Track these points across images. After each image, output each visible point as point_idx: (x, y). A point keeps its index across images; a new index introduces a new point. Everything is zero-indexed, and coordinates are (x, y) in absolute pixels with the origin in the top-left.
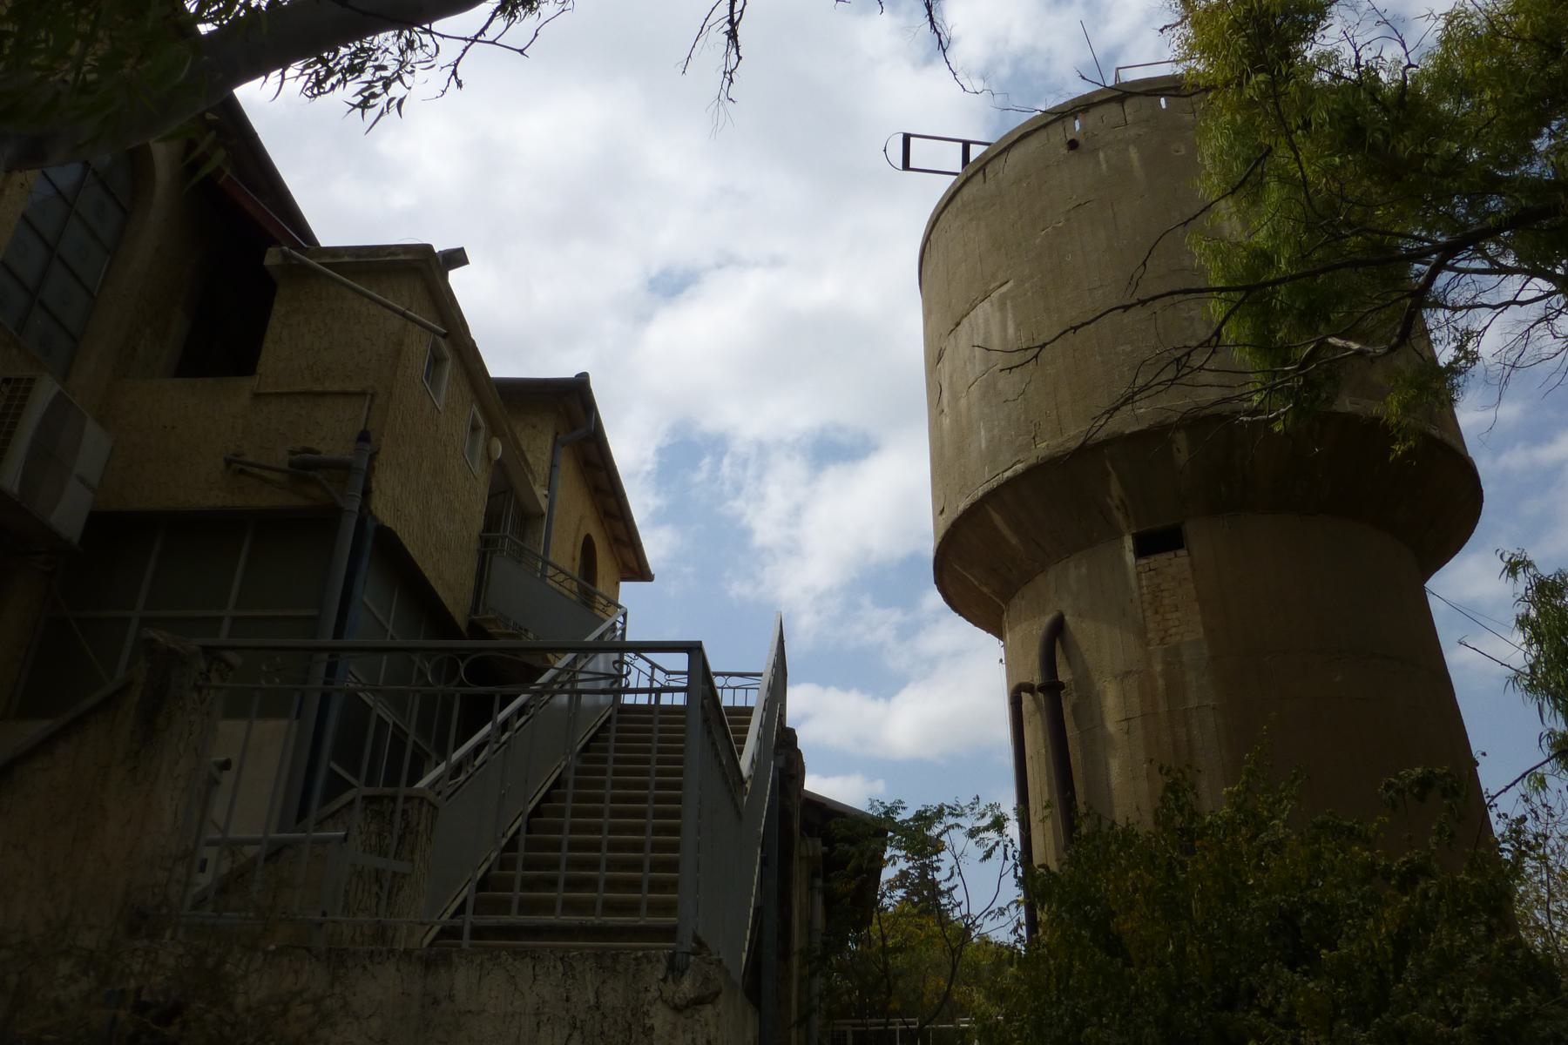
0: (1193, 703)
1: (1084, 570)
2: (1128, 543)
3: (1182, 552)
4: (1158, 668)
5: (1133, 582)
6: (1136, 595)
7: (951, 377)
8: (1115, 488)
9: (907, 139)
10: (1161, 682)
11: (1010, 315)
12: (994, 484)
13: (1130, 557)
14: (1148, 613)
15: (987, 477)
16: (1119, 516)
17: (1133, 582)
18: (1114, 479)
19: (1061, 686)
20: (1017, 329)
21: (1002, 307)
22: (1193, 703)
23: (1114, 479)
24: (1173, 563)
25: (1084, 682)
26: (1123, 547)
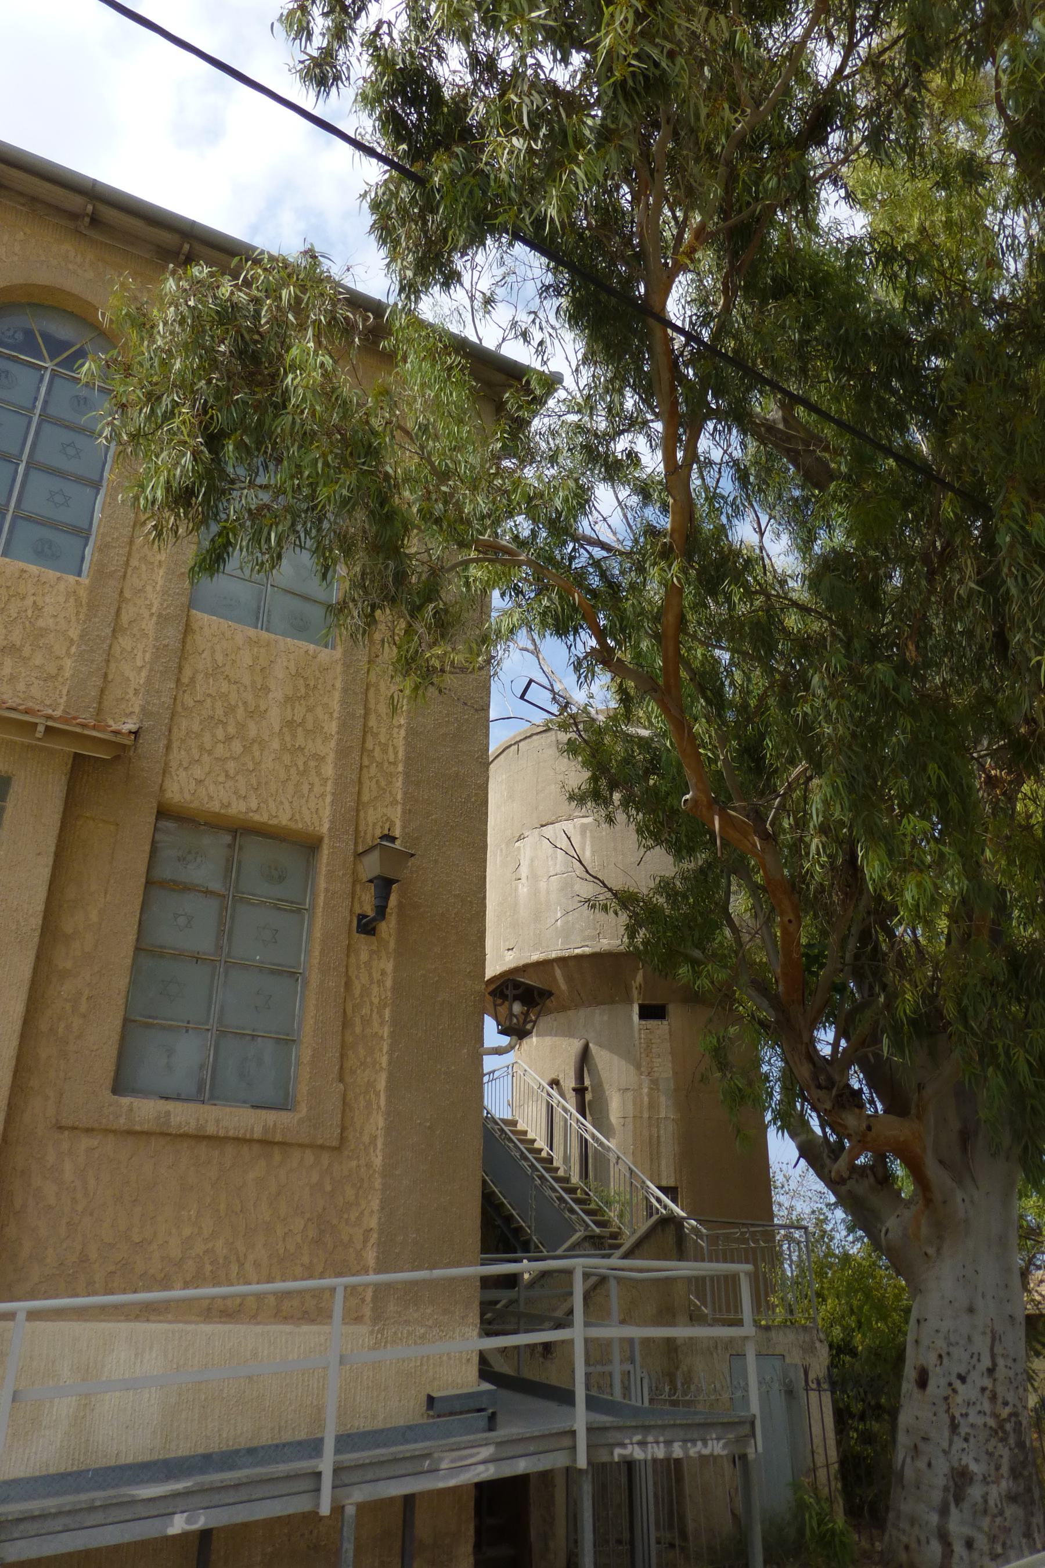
0: (663, 1115)
1: (606, 1018)
2: (636, 1009)
3: (665, 1022)
4: (646, 1090)
5: (636, 1035)
6: (637, 1042)
7: (532, 860)
8: (639, 977)
9: (531, 681)
10: (646, 1099)
11: (588, 842)
12: (566, 954)
13: (636, 1017)
14: (643, 1055)
15: (560, 947)
16: (635, 993)
17: (636, 1035)
18: (641, 972)
19: (586, 1089)
20: (593, 853)
21: (583, 833)
22: (663, 1115)
23: (641, 972)
24: (660, 1027)
25: (598, 1087)
26: (632, 1010)
